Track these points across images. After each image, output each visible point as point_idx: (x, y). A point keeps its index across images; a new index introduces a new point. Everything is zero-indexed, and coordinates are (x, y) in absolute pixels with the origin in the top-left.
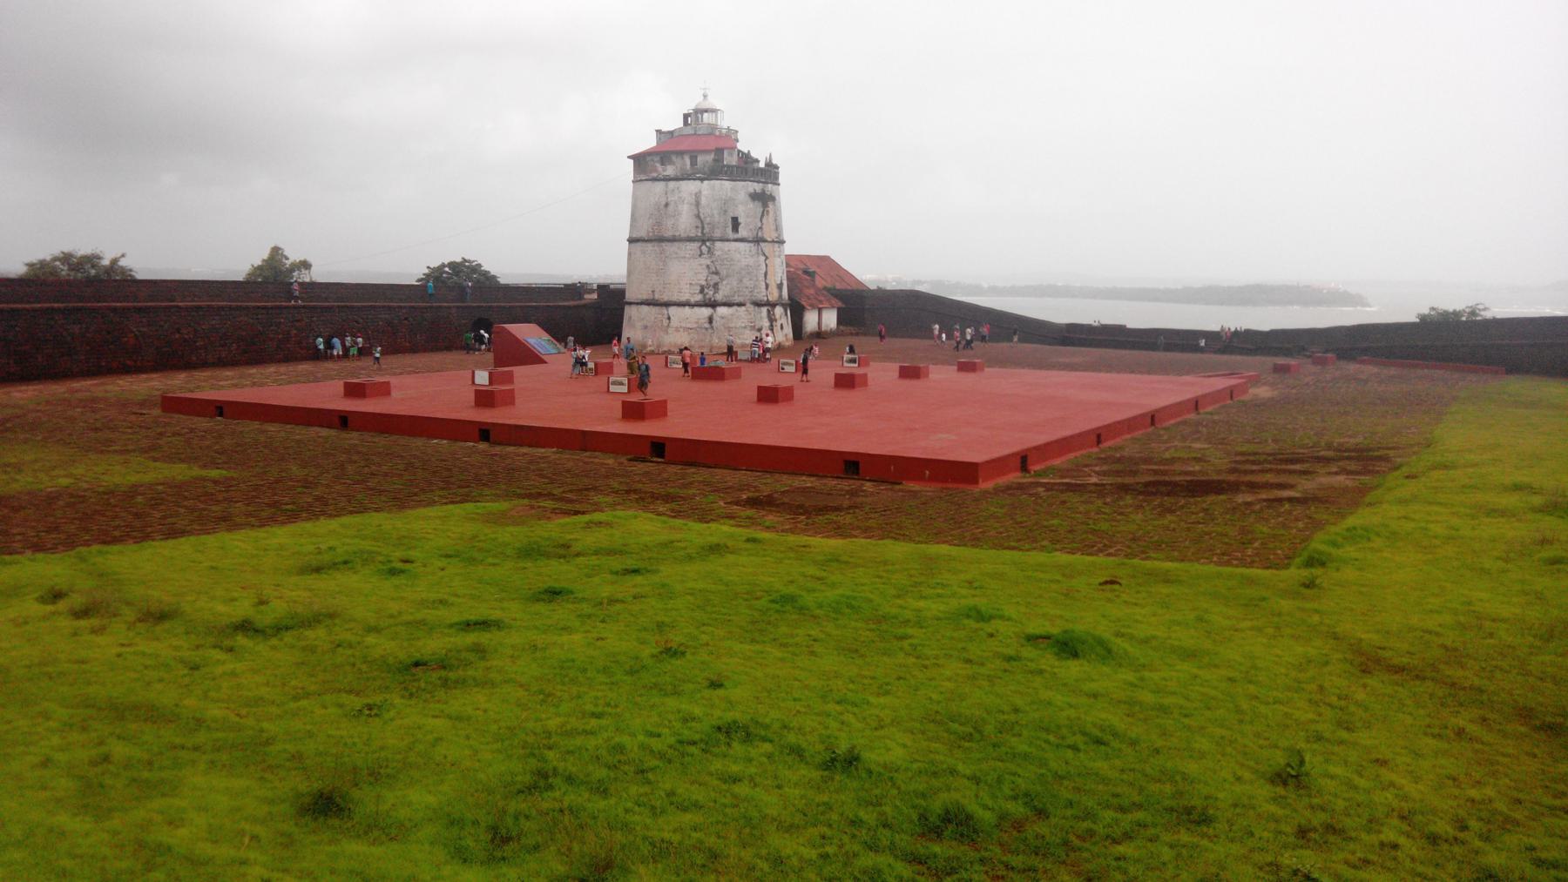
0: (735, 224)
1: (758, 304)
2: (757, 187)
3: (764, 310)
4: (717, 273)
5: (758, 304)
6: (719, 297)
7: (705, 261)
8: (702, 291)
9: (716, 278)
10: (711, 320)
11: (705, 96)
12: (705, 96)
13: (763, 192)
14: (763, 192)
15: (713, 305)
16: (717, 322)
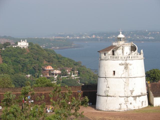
2: (123, 62)
4: (109, 87)
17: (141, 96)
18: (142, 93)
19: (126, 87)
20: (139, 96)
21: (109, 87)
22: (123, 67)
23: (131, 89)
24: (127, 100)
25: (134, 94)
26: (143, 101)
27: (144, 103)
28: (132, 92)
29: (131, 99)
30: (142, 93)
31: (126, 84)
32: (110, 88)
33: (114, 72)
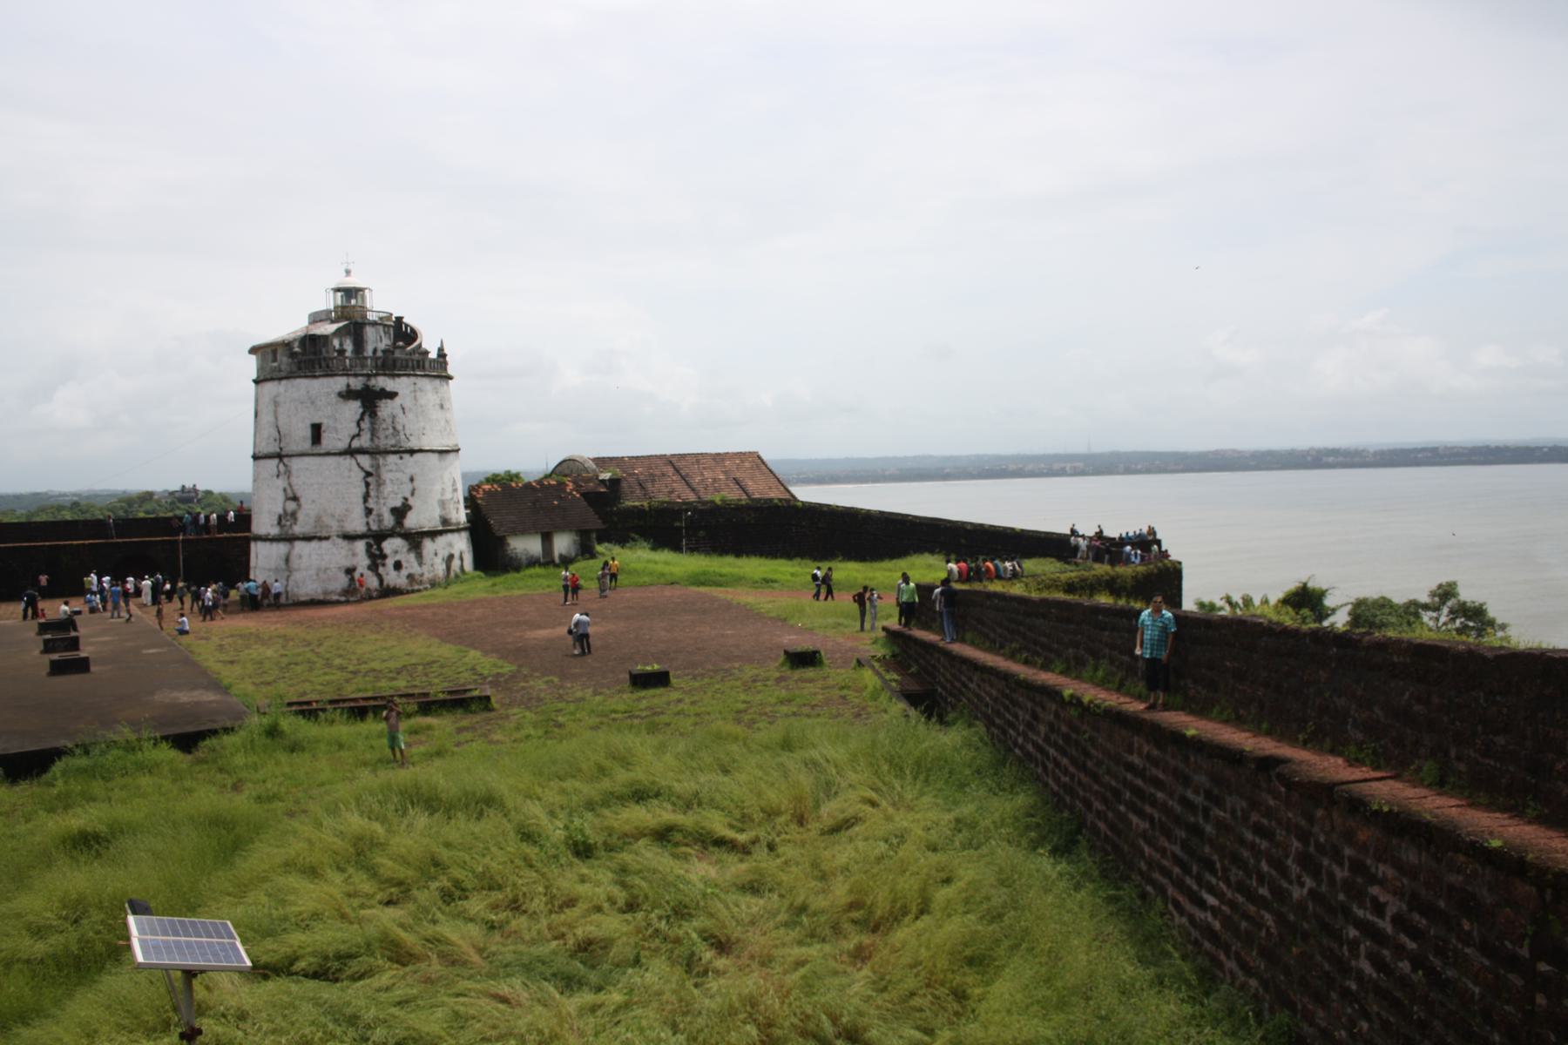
0: (317, 430)
1: (350, 537)
2: (357, 383)
3: (360, 546)
5: (350, 537)
6: (298, 529)
7: (281, 483)
8: (279, 523)
9: (291, 506)
10: (287, 560)
11: (348, 272)
12: (348, 272)
13: (367, 388)
14: (367, 388)
15: (290, 539)
16: (295, 562)
17: (441, 533)
18: (445, 521)
19: (372, 493)
20: (433, 534)
21: (295, 499)
22: (355, 407)
23: (398, 503)
24: (380, 549)
25: (411, 521)
26: (451, 557)
27: (456, 563)
28: (400, 512)
29: (394, 547)
30: (445, 521)
31: (371, 478)
32: (303, 501)
33: (317, 430)
